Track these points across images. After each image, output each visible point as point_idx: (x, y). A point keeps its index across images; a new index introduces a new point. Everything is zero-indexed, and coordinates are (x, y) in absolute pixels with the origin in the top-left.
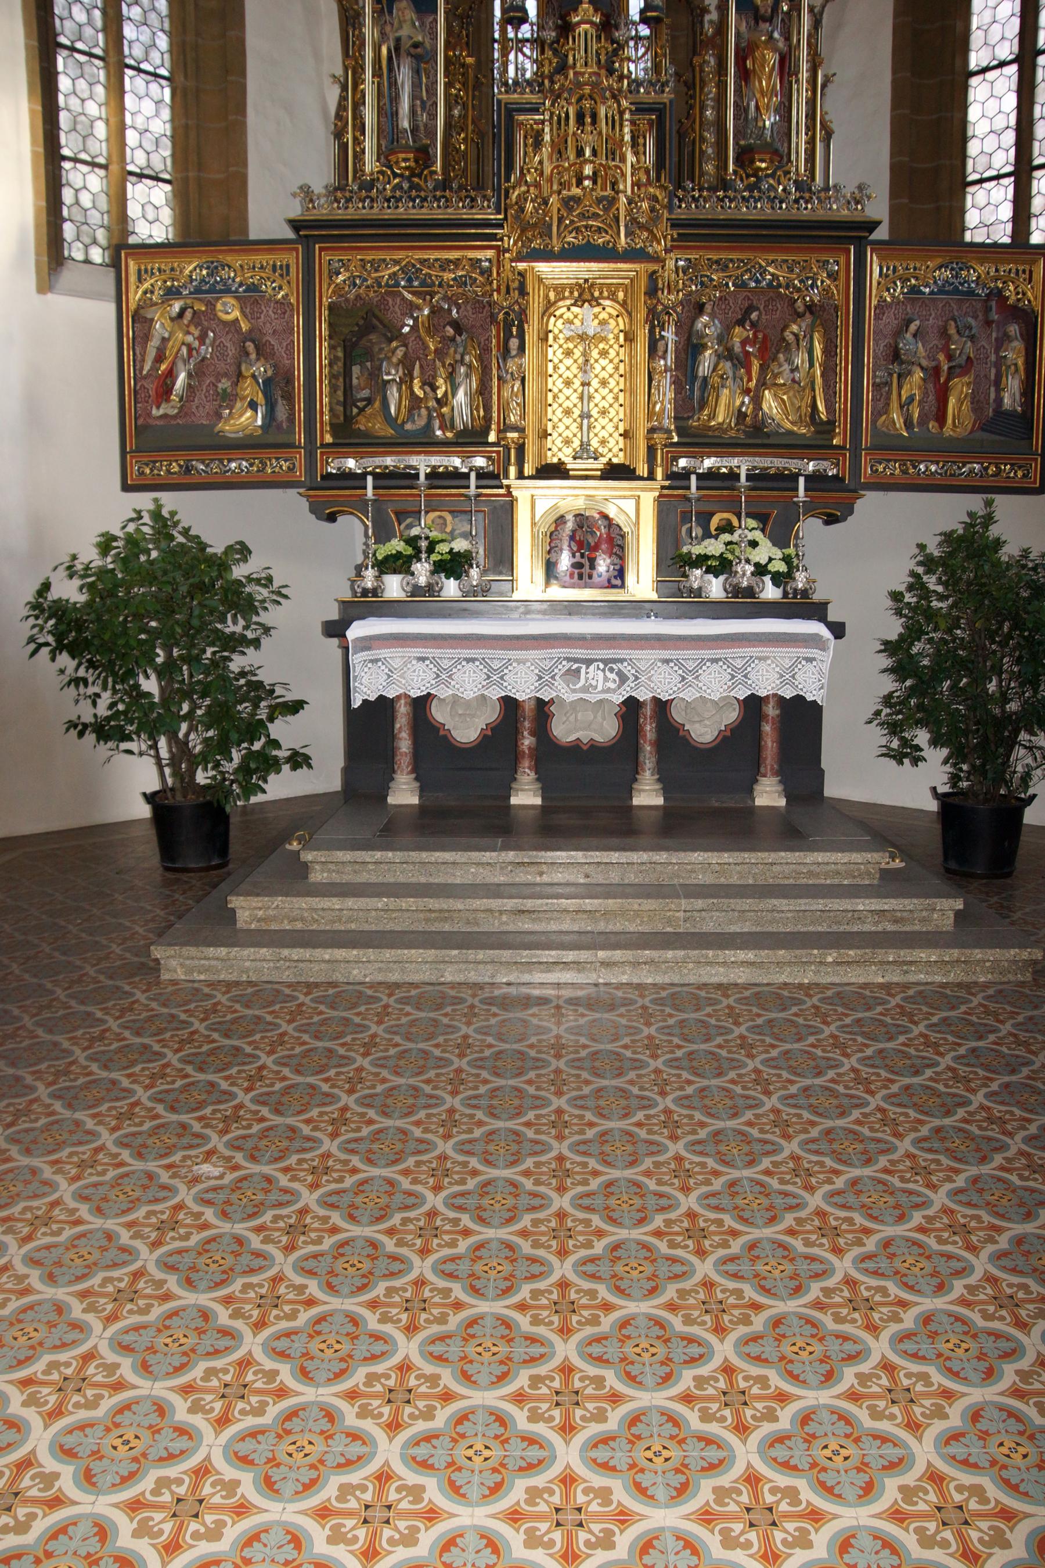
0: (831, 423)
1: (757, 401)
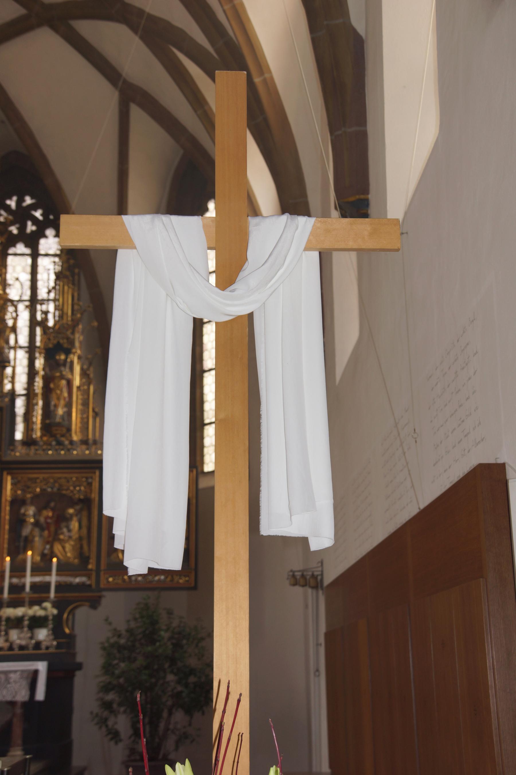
0: (88, 558)
1: (52, 547)
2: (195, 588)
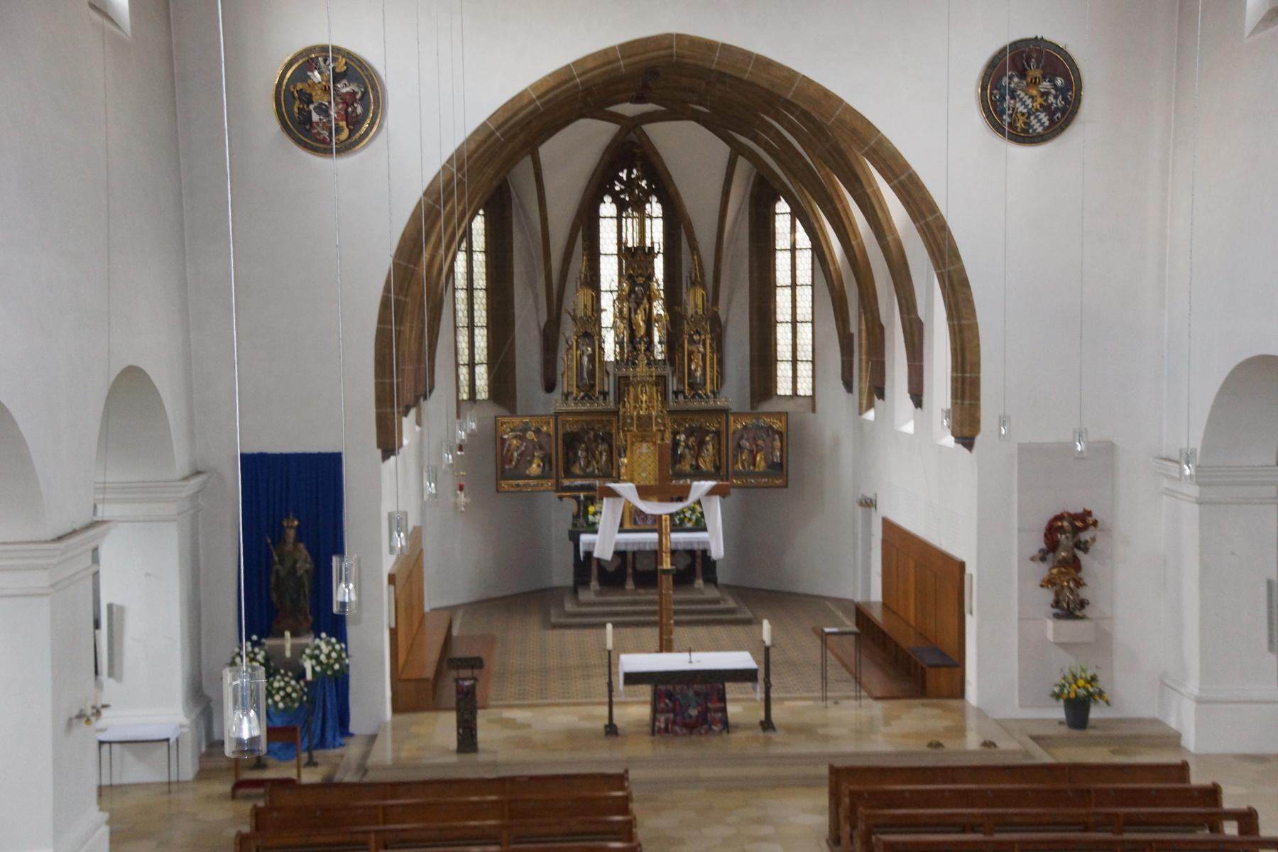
1: (697, 461)
2: (787, 486)
